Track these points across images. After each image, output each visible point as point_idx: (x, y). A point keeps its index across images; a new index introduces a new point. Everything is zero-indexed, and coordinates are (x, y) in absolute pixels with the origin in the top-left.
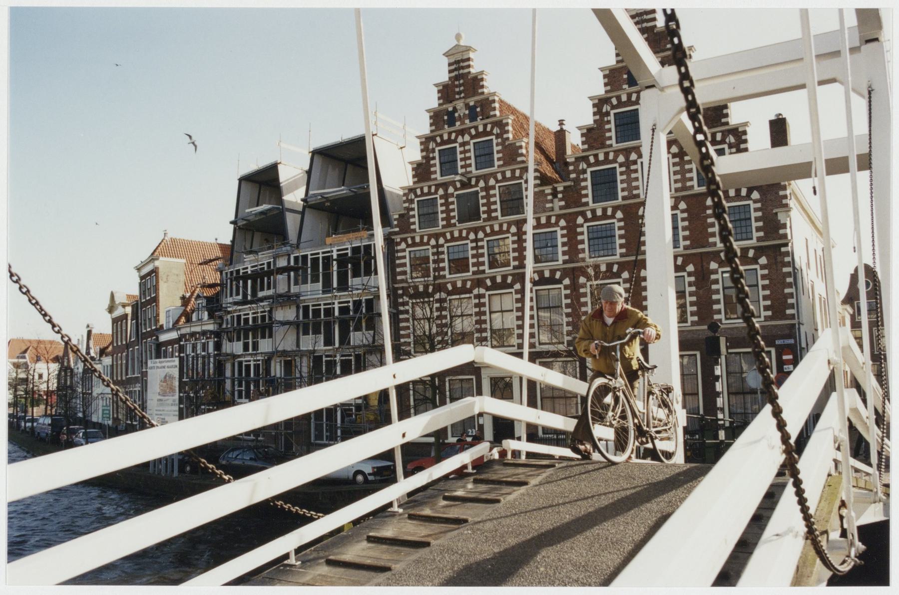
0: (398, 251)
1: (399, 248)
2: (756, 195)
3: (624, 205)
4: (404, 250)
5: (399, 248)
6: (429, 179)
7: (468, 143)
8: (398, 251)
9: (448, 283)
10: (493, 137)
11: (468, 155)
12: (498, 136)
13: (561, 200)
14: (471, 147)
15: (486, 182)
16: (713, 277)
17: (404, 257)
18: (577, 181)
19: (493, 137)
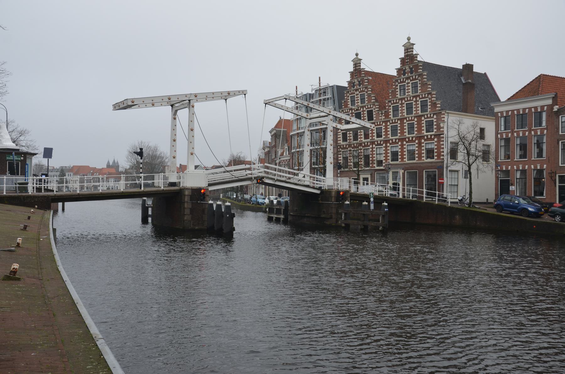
0: (338, 132)
1: (339, 131)
2: (435, 117)
3: (401, 119)
4: (340, 132)
5: (339, 131)
6: (348, 107)
8: (338, 132)
9: (375, 141)
10: (365, 93)
11: (358, 99)
12: (366, 92)
13: (383, 116)
14: (359, 96)
15: (363, 109)
16: (423, 145)
17: (340, 135)
18: (389, 109)
19: (365, 93)
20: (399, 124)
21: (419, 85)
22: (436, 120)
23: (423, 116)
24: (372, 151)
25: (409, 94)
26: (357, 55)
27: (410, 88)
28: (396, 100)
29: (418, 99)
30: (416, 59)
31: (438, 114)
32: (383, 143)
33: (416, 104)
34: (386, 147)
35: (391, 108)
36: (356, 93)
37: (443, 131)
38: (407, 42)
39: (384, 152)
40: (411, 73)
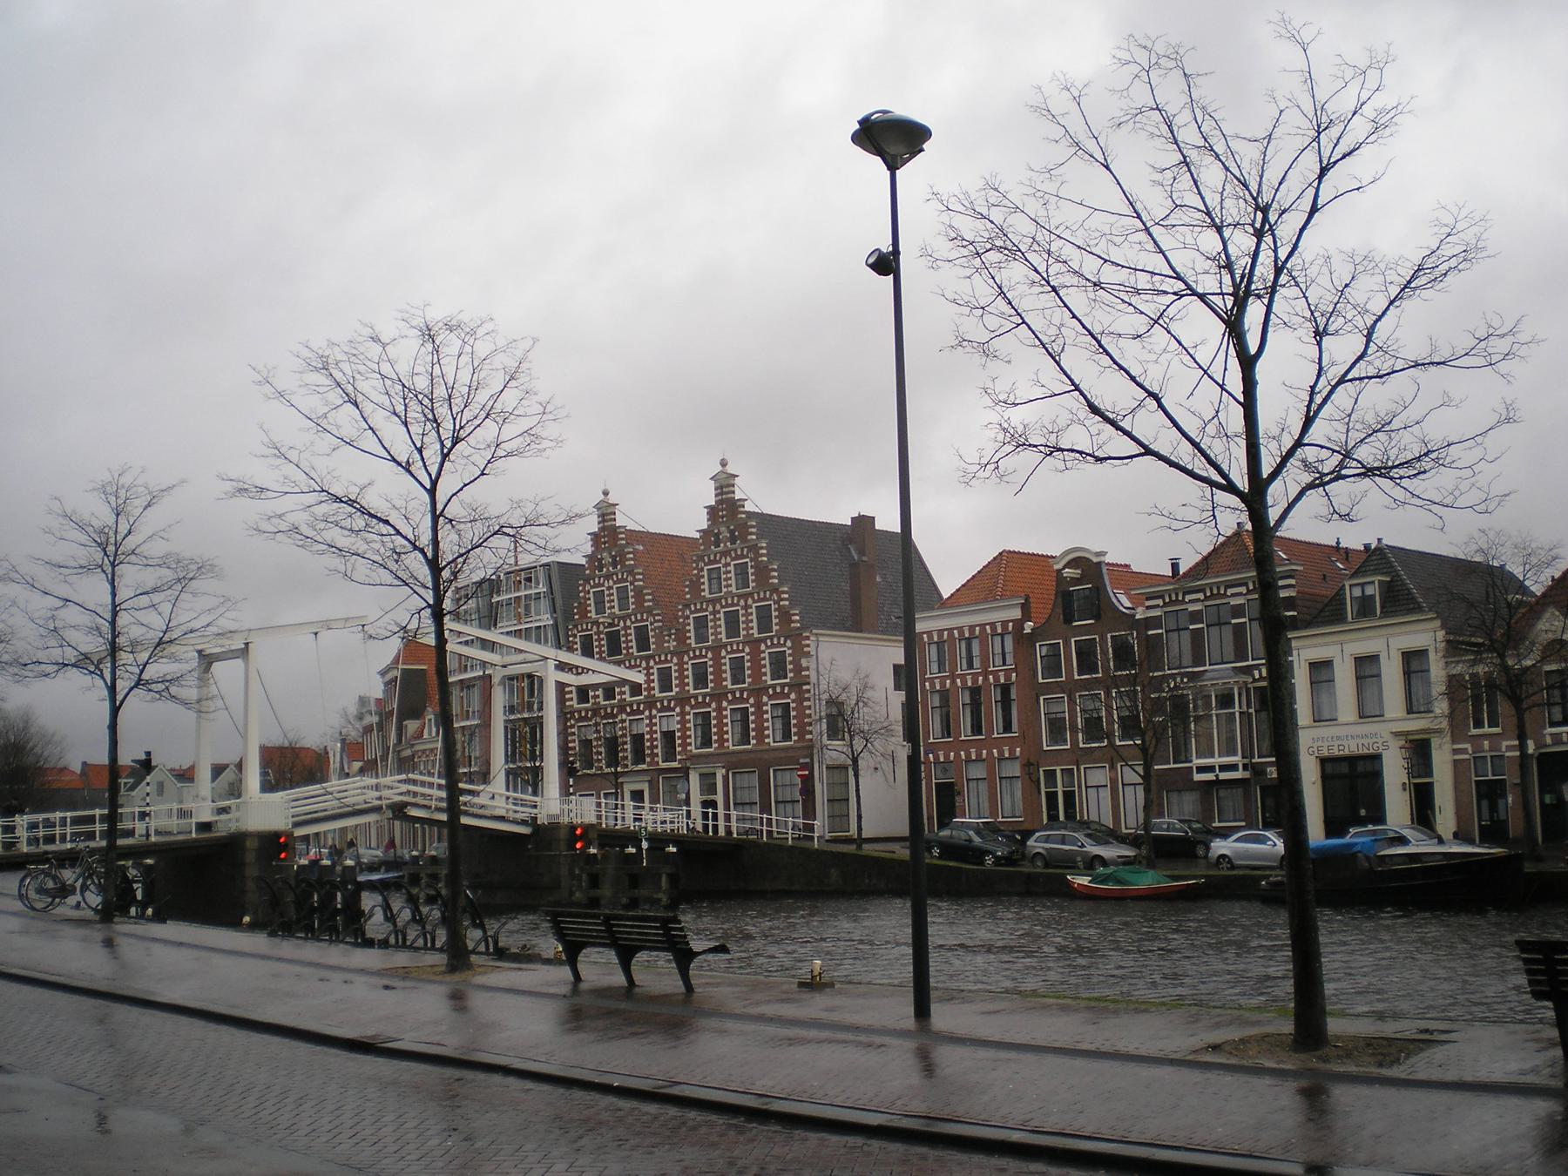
7: (611, 588)
12: (632, 583)
13: (674, 640)
14: (614, 591)
16: (765, 708)
20: (711, 659)
21: (751, 571)
22: (790, 651)
23: (764, 640)
24: (651, 725)
25: (730, 589)
26: (606, 493)
27: (732, 575)
28: (702, 603)
29: (750, 601)
30: (742, 509)
31: (797, 637)
32: (675, 706)
33: (747, 614)
34: (683, 714)
35: (691, 621)
36: (606, 584)
37: (808, 676)
38: (721, 471)
39: (679, 726)
40: (733, 540)
